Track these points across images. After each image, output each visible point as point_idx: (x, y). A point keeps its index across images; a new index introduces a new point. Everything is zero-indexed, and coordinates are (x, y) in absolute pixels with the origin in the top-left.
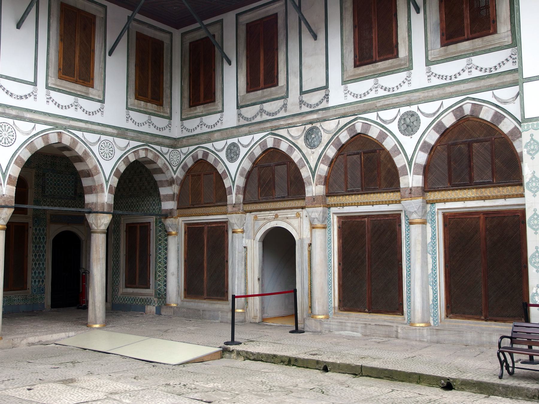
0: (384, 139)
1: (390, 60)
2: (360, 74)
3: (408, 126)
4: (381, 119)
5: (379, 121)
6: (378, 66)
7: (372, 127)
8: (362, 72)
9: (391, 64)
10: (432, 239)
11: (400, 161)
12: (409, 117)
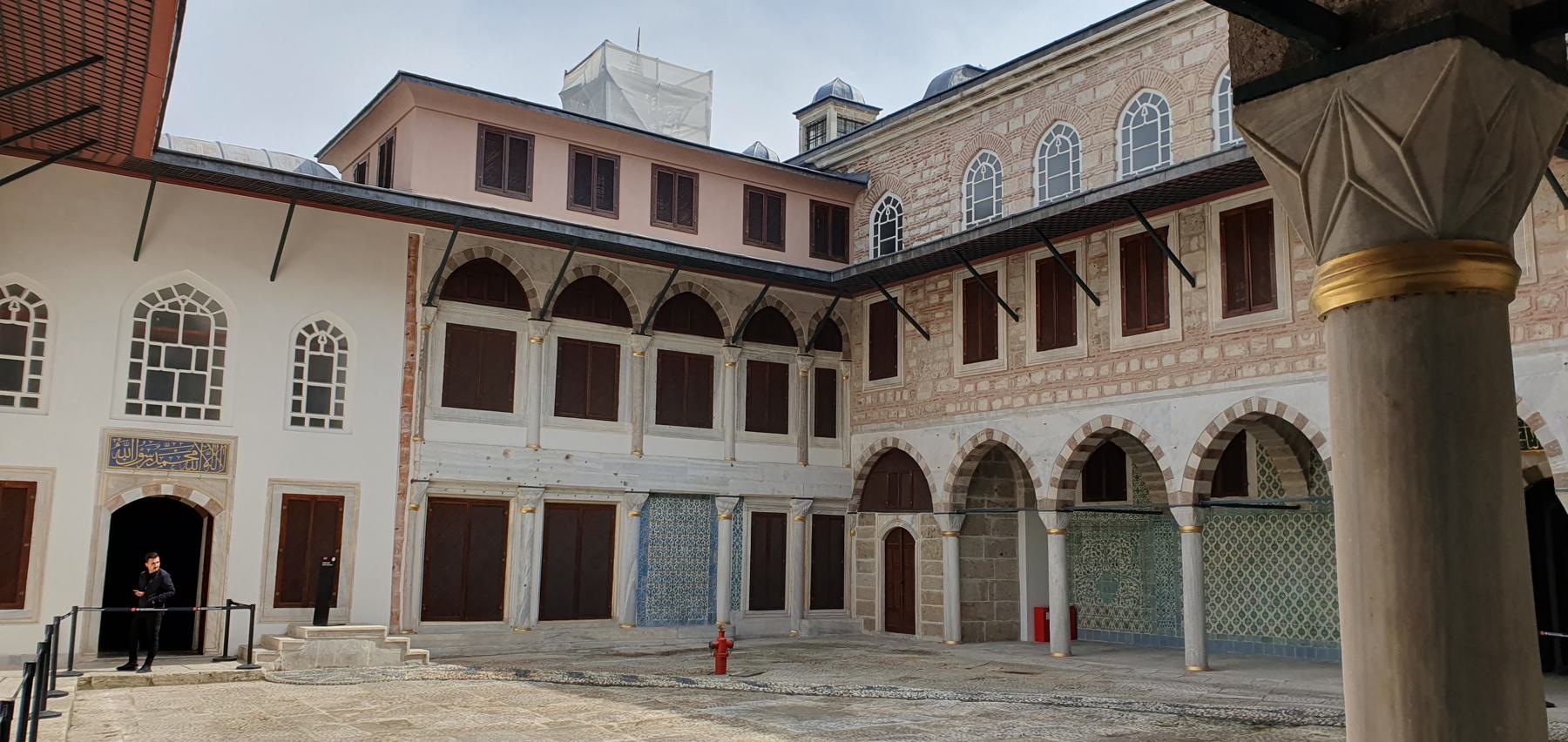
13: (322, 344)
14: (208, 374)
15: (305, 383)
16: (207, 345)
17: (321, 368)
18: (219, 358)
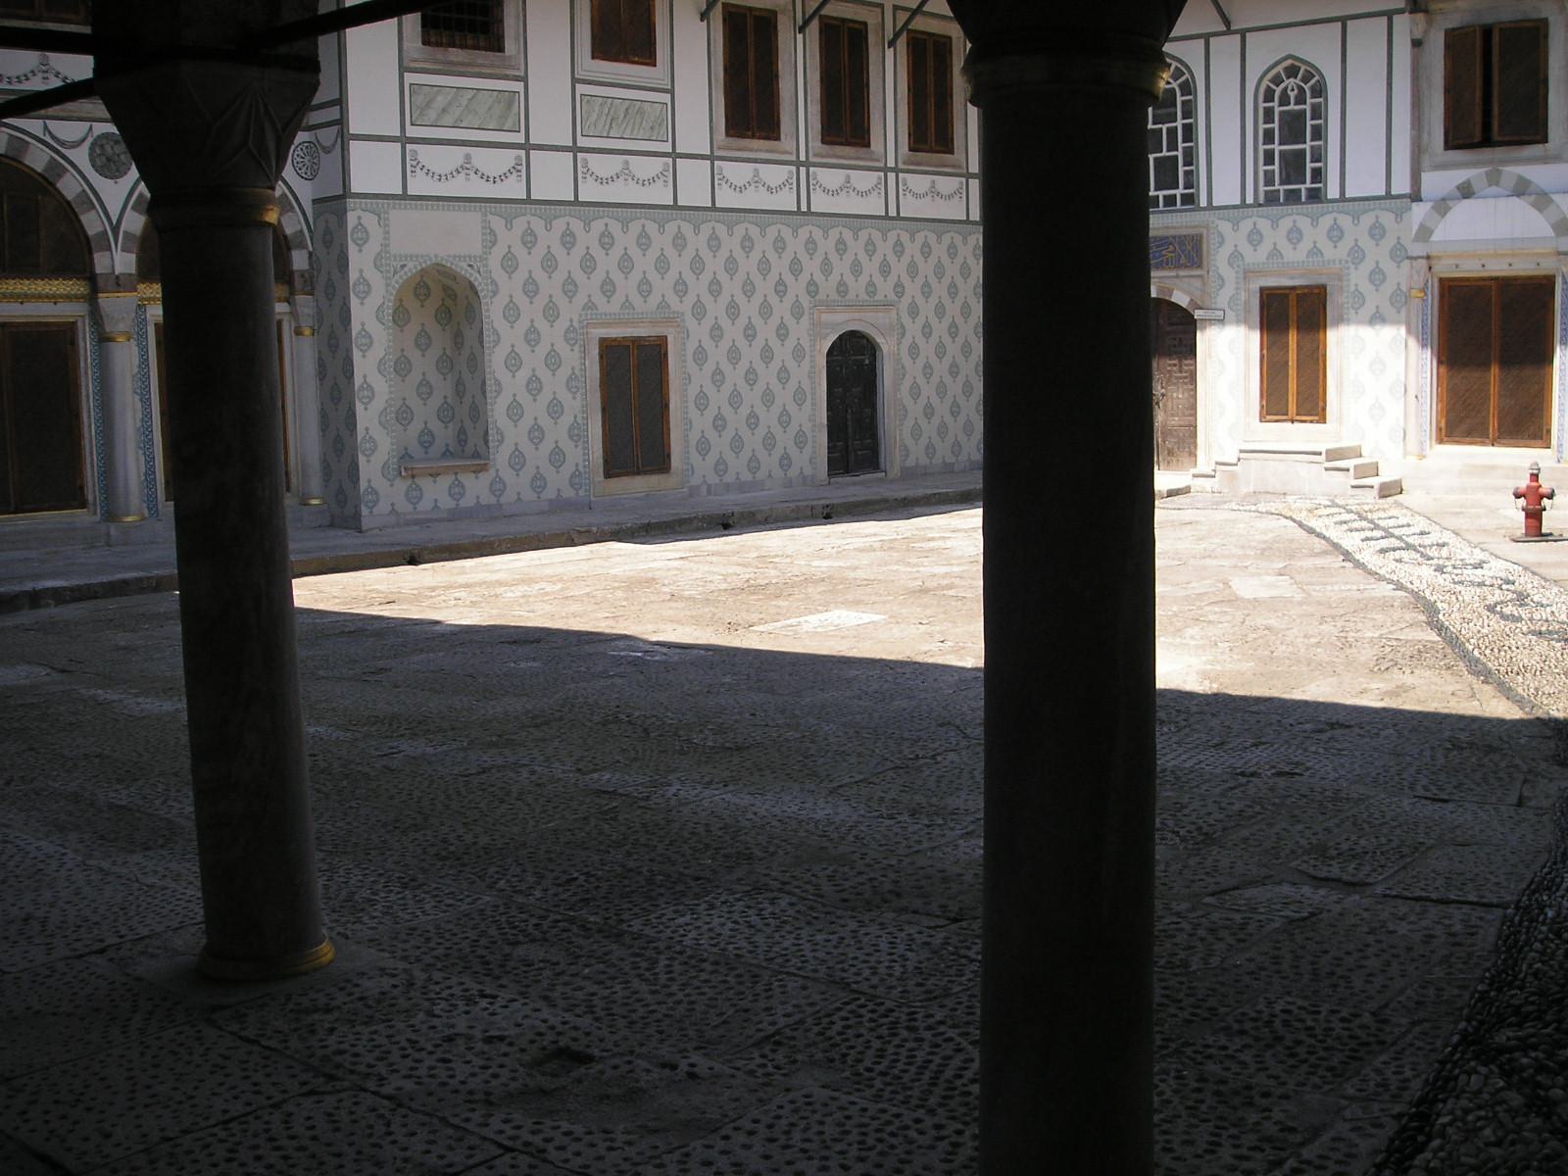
0: (60, 176)
3: (109, 160)
4: (53, 137)
5: (48, 139)
11: (92, 224)
12: (112, 143)
13: (1292, 95)
14: (1180, 154)
15: (1277, 148)
16: (1175, 121)
17: (1293, 128)
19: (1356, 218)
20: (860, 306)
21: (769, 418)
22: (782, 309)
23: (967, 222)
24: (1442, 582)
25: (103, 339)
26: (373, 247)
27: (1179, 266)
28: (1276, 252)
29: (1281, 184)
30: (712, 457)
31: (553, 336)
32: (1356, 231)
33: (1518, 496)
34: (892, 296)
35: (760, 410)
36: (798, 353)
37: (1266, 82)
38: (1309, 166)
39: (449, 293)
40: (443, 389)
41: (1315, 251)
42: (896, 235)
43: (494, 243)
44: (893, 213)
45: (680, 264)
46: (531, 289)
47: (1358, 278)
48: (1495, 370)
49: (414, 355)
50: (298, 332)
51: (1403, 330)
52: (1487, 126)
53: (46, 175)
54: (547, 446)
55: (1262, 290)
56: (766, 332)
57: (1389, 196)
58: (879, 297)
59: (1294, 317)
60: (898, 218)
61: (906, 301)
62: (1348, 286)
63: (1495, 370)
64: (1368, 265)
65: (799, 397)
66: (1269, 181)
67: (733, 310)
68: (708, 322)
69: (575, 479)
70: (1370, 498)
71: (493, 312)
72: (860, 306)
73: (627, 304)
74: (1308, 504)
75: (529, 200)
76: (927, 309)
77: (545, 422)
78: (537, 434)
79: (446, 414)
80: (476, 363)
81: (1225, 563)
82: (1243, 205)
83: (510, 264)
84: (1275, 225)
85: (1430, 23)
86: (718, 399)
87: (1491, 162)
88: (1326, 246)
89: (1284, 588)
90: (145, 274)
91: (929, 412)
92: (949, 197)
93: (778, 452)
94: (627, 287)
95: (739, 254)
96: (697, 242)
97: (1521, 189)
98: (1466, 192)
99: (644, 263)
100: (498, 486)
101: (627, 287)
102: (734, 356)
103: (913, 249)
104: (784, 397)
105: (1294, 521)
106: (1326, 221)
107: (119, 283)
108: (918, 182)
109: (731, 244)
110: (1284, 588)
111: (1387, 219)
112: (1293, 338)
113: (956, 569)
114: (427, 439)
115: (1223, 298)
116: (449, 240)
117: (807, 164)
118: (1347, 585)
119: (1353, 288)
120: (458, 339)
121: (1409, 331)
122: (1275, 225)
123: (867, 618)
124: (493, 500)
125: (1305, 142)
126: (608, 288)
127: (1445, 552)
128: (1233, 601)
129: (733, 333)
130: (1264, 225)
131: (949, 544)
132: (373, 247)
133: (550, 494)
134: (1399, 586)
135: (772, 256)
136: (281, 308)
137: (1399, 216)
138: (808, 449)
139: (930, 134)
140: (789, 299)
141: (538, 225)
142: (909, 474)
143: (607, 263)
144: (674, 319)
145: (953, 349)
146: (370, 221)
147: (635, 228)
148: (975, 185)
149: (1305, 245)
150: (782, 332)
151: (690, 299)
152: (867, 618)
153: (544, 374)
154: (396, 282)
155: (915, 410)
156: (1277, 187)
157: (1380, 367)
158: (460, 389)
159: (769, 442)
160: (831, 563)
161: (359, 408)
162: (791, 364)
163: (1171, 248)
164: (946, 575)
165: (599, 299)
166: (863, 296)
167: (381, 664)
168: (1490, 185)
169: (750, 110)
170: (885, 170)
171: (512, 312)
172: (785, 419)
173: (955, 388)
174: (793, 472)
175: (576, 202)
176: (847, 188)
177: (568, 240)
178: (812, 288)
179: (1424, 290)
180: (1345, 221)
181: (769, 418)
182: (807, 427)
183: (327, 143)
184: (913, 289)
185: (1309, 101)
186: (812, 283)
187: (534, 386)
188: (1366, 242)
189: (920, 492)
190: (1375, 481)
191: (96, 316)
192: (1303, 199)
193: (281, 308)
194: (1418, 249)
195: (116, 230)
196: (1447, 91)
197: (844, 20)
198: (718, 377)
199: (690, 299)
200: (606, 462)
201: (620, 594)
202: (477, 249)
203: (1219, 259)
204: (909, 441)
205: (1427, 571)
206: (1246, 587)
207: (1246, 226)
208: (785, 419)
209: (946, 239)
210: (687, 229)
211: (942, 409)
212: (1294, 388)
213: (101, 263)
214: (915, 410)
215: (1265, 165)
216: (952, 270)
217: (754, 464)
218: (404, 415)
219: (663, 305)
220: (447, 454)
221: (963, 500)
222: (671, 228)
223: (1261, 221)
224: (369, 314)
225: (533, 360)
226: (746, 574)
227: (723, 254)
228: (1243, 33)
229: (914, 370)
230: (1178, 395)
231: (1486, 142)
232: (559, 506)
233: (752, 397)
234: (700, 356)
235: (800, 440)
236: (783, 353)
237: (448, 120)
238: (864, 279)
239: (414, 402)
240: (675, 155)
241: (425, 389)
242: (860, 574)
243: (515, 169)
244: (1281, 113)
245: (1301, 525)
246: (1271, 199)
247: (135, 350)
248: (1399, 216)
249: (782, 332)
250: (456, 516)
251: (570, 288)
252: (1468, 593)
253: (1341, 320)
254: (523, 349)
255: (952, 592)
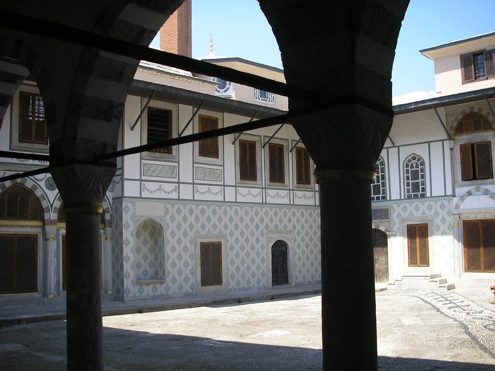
0: (36, 190)
1: (43, 145)
2: (23, 147)
3: (51, 185)
6: (35, 146)
7: (28, 181)
8: (24, 146)
9: (43, 147)
10: (57, 248)
11: (45, 204)
13: (414, 165)
14: (380, 184)
15: (410, 181)
17: (415, 175)
18: (383, 177)
19: (436, 202)
20: (282, 232)
21: (253, 268)
22: (257, 233)
23: (315, 205)
24: (469, 318)
25: (46, 239)
26: (130, 213)
27: (381, 219)
28: (411, 214)
29: (412, 193)
30: (235, 280)
31: (186, 241)
32: (436, 206)
33: (492, 289)
34: (292, 229)
35: (251, 265)
36: (263, 247)
37: (406, 162)
38: (421, 187)
39: (154, 228)
40: (151, 257)
41: (424, 213)
42: (294, 211)
43: (168, 212)
44: (292, 203)
45: (226, 219)
46: (179, 226)
47: (437, 221)
48: (482, 249)
49: (142, 247)
50: (106, 239)
51: (452, 237)
52: (474, 174)
53: (32, 189)
54: (183, 276)
55: (408, 225)
56: (253, 240)
57: (445, 195)
58: (288, 229)
59: (418, 233)
60: (294, 205)
61: (296, 230)
62: (434, 224)
63: (482, 249)
64: (440, 217)
65: (263, 261)
66: (408, 192)
67: (242, 234)
68: (234, 237)
69: (192, 286)
70: (444, 290)
71: (167, 234)
72: (282, 232)
73: (209, 232)
74: (425, 293)
75: (179, 199)
76: (303, 233)
77: (183, 268)
78: (180, 272)
79: (152, 265)
80: (161, 250)
81: (399, 313)
82: (401, 199)
83: (173, 219)
84: (411, 205)
85: (455, 143)
86: (237, 262)
87: (477, 184)
88: (427, 211)
89: (418, 321)
90: (60, 220)
91: (304, 265)
92: (310, 198)
93: (256, 278)
94: (209, 226)
95: (244, 216)
96: (231, 212)
97: (486, 193)
98: (469, 194)
99: (215, 219)
100: (168, 288)
101: (209, 226)
102: (242, 248)
103: (298, 214)
104: (258, 261)
105: (421, 298)
106: (427, 204)
107: (52, 223)
108: (300, 193)
109: (242, 213)
110: (418, 321)
111: (445, 203)
112: (418, 240)
113: (313, 316)
114: (145, 273)
115: (395, 228)
116: (154, 211)
117: (265, 188)
118: (438, 320)
119: (436, 224)
120: (156, 242)
121: (454, 237)
122: (411, 205)
123: (285, 333)
124: (166, 293)
125: (419, 180)
126: (203, 226)
127: (469, 308)
128: (402, 326)
129: (242, 241)
130: (407, 205)
131: (310, 308)
132: (130, 213)
133: (184, 291)
134: (455, 320)
135: (254, 217)
136: (102, 231)
137: (449, 201)
138: (266, 278)
139: (303, 179)
140: (260, 230)
141: (182, 207)
142: (298, 285)
143: (203, 219)
144: (224, 237)
145: (311, 245)
146: (130, 205)
147: (212, 208)
148: (317, 194)
149: (421, 211)
150: (258, 241)
151: (229, 230)
152: (285, 333)
153: (183, 253)
154: (137, 224)
155: (299, 265)
156: (411, 194)
157: (446, 249)
158: (156, 258)
159: (254, 275)
160: (273, 314)
161: (125, 263)
162: (260, 250)
163: (379, 213)
164: (310, 318)
165: (200, 230)
166: (283, 229)
167: (129, 346)
168: (477, 192)
169: (248, 172)
170: (289, 190)
171: (173, 234)
172: (258, 268)
173: (312, 258)
174: (261, 285)
175: (194, 200)
176: (277, 195)
177: (191, 211)
178: (267, 227)
179: (458, 224)
180: (432, 203)
181: (253, 268)
182: (265, 271)
183: (117, 181)
184: (298, 227)
185: (420, 167)
186: (267, 225)
187: (180, 257)
188: (439, 210)
189: (301, 291)
190: (446, 285)
191: (44, 232)
192: (419, 197)
193: (102, 231)
194: (455, 212)
195: (52, 206)
196: (462, 163)
197: (276, 144)
198: (237, 255)
199: (229, 230)
200: (202, 281)
201: (206, 324)
202: (162, 213)
203: (394, 216)
204: (297, 274)
205: (464, 315)
206: (406, 321)
207: (402, 206)
208: (258, 268)
209: (309, 211)
210: (228, 208)
211: (308, 264)
212: (419, 256)
213: (46, 216)
214: (299, 265)
215: (407, 187)
216: (310, 221)
217: (249, 282)
218: (138, 265)
219: (220, 232)
220: (152, 278)
221: (315, 293)
222: (223, 208)
223: (406, 204)
224: (128, 234)
225: (179, 249)
226: (246, 318)
227: (239, 216)
228: (398, 147)
229: (299, 252)
230: (382, 259)
231: (475, 178)
232: (187, 295)
233: (248, 261)
234: (232, 248)
235: (263, 274)
236: (258, 247)
237: (155, 174)
238: (283, 224)
239: (142, 261)
240: (224, 186)
241: (145, 257)
242: (282, 318)
243: (175, 189)
244: (411, 171)
245: (423, 300)
246: (409, 197)
247: (56, 243)
248: (449, 201)
249: (258, 241)
250: (155, 297)
251: (191, 226)
252: (478, 322)
253: (433, 234)
254: (176, 245)
255: (312, 324)
